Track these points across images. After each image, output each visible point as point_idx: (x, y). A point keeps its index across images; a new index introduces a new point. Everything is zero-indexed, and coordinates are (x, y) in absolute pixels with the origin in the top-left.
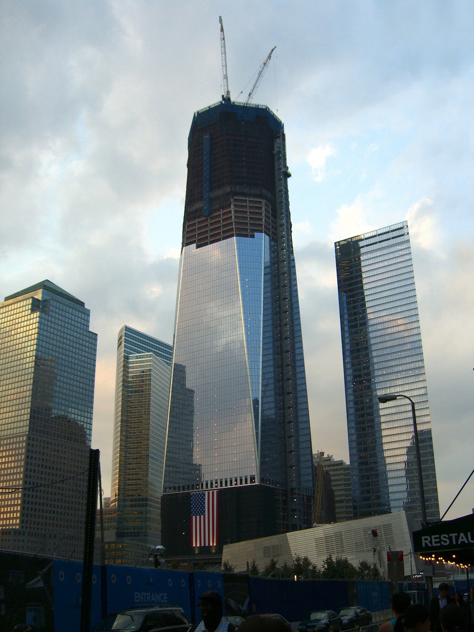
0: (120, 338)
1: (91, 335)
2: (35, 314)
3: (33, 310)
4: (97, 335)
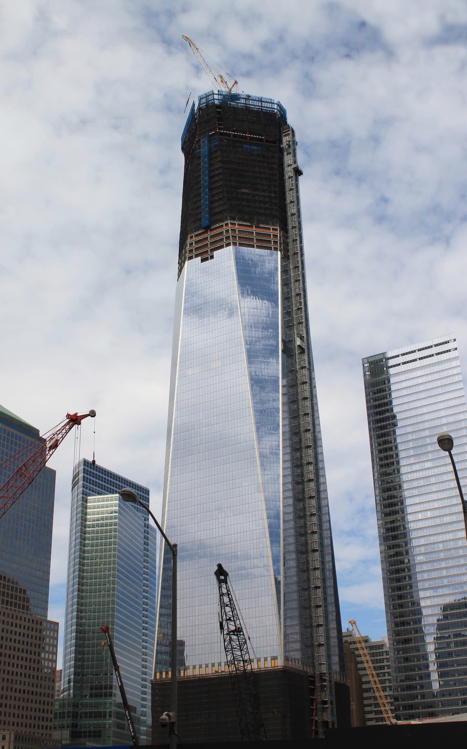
0: (78, 474)
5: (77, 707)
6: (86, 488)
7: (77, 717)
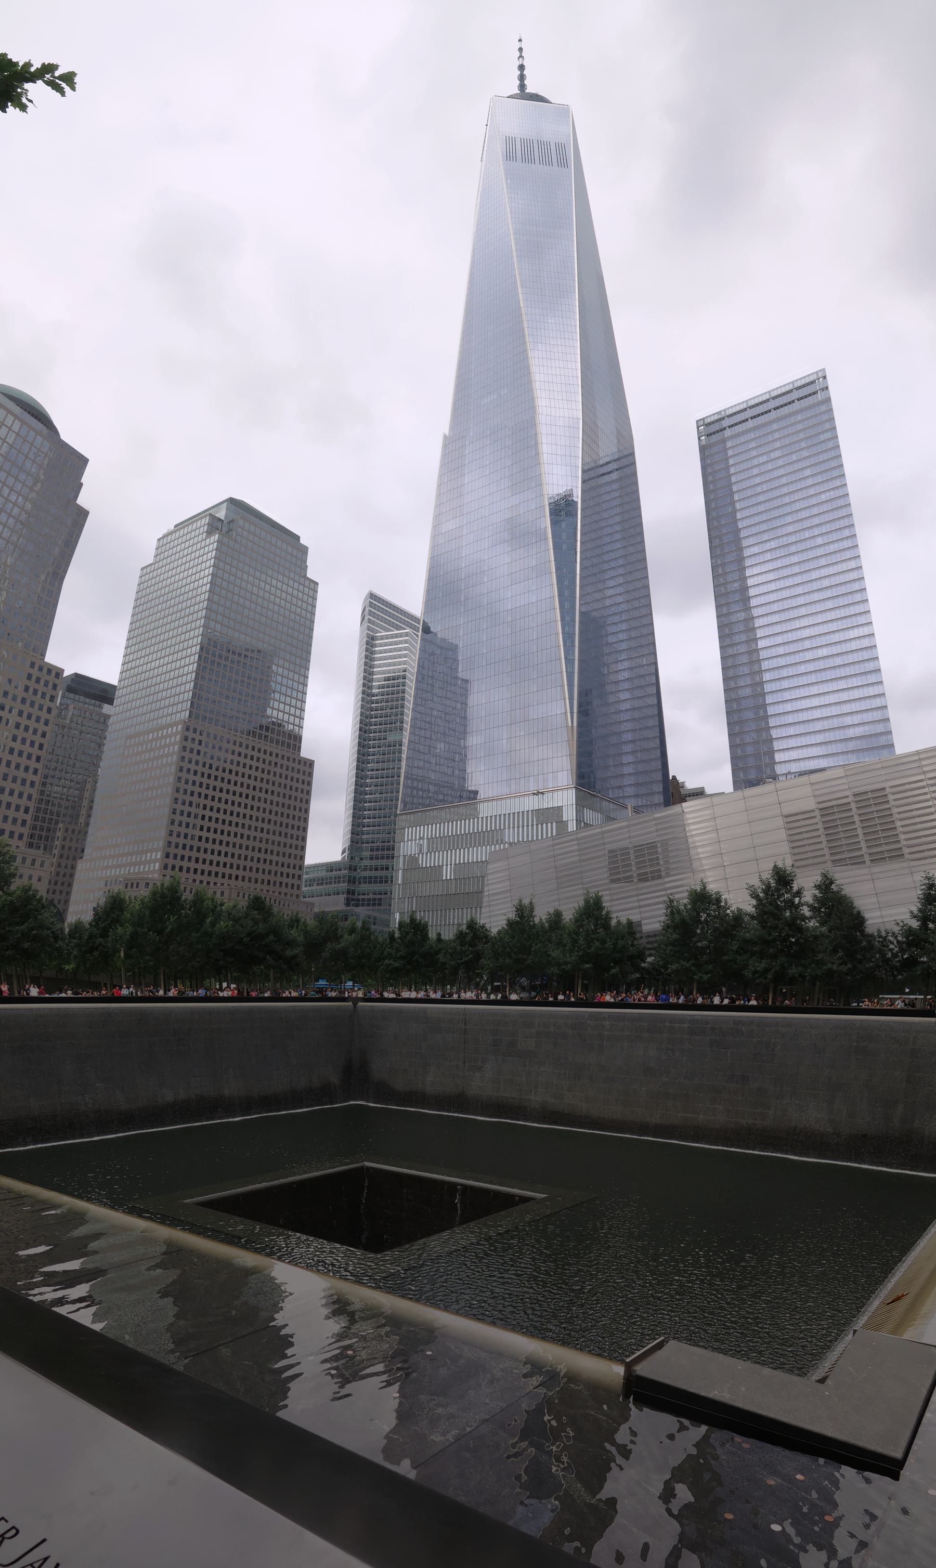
2: (212, 538)
3: (209, 533)
4: (317, 584)
5: (355, 870)
7: (354, 883)
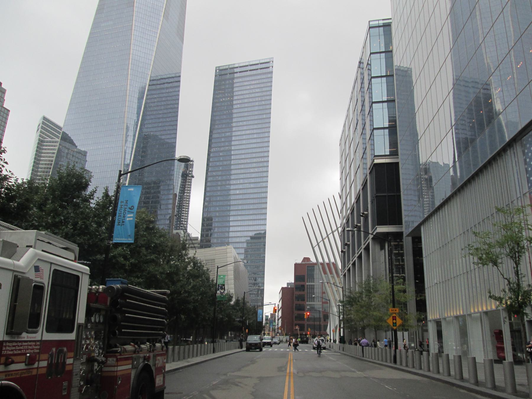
0: (39, 125)
1: (3, 110)
4: (9, 111)
6: (43, 134)
